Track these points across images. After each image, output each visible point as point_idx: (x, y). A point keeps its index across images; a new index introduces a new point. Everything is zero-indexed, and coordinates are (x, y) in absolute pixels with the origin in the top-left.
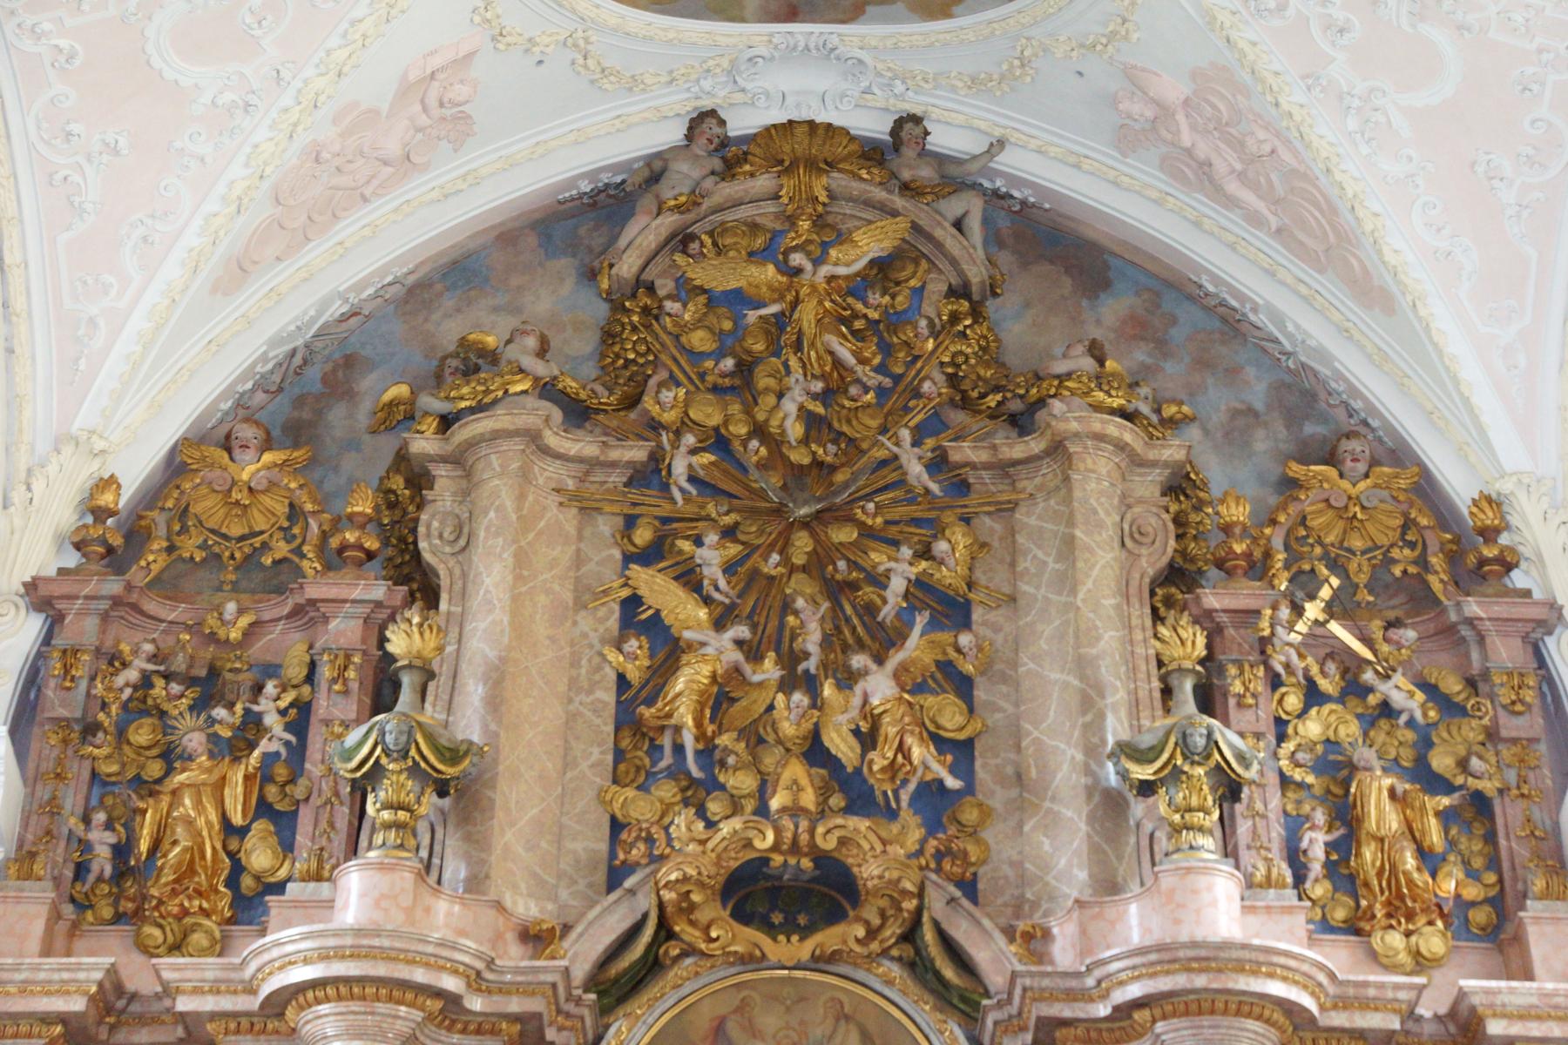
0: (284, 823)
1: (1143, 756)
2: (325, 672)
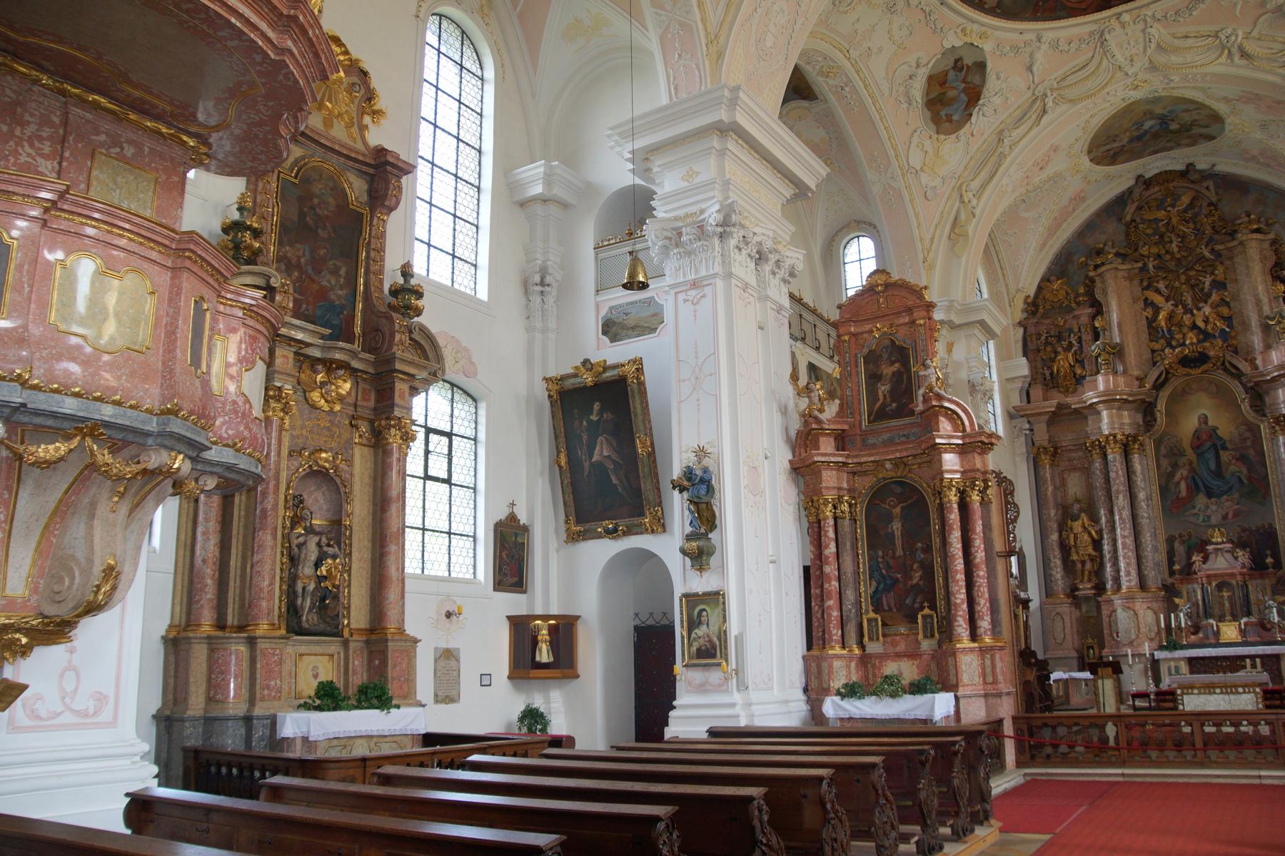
0: (1081, 362)
1: (1272, 319)
2: (1083, 330)
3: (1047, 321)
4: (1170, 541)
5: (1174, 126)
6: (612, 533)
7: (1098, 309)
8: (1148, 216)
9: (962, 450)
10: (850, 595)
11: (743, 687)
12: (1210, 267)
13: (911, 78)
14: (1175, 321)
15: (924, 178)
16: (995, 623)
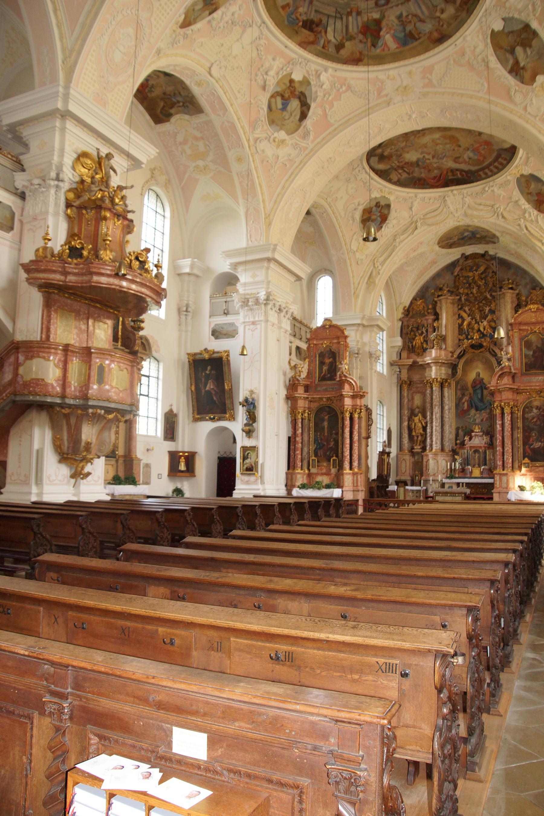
0: (426, 341)
3: (413, 320)
4: (457, 429)
5: (478, 236)
6: (212, 420)
7: (437, 317)
8: (465, 274)
9: (353, 397)
10: (306, 449)
11: (263, 483)
12: (489, 303)
13: (355, 209)
14: (471, 326)
15: (358, 255)
16: (359, 464)
